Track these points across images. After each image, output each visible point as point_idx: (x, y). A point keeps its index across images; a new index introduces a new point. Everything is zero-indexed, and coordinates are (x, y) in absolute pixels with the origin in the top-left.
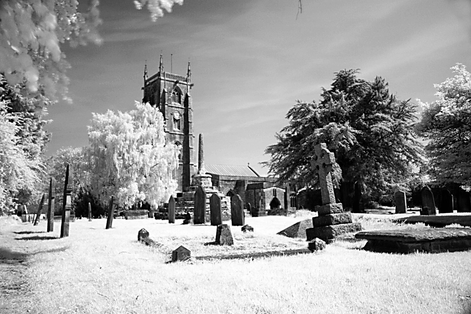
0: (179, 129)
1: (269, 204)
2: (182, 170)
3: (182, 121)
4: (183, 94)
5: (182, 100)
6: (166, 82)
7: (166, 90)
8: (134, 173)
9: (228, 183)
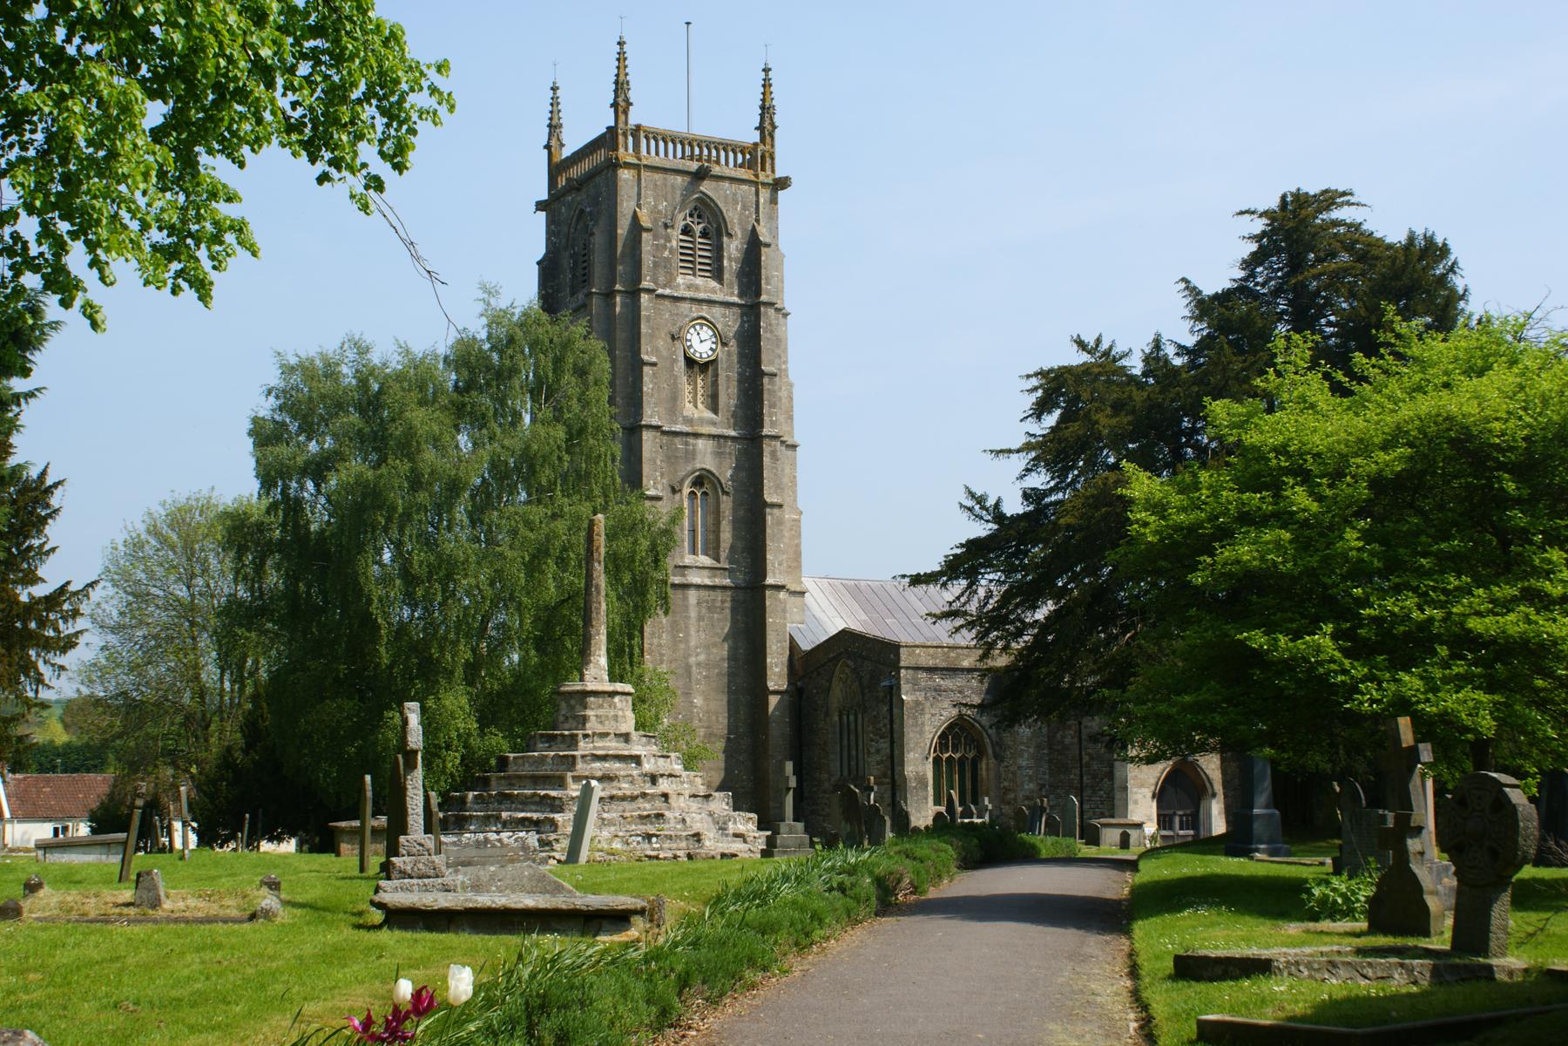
0: (715, 410)
1: (1147, 792)
2: (728, 611)
3: (729, 368)
4: (737, 230)
5: (731, 265)
6: (645, 174)
7: (645, 221)
8: (455, 643)
9: (947, 683)
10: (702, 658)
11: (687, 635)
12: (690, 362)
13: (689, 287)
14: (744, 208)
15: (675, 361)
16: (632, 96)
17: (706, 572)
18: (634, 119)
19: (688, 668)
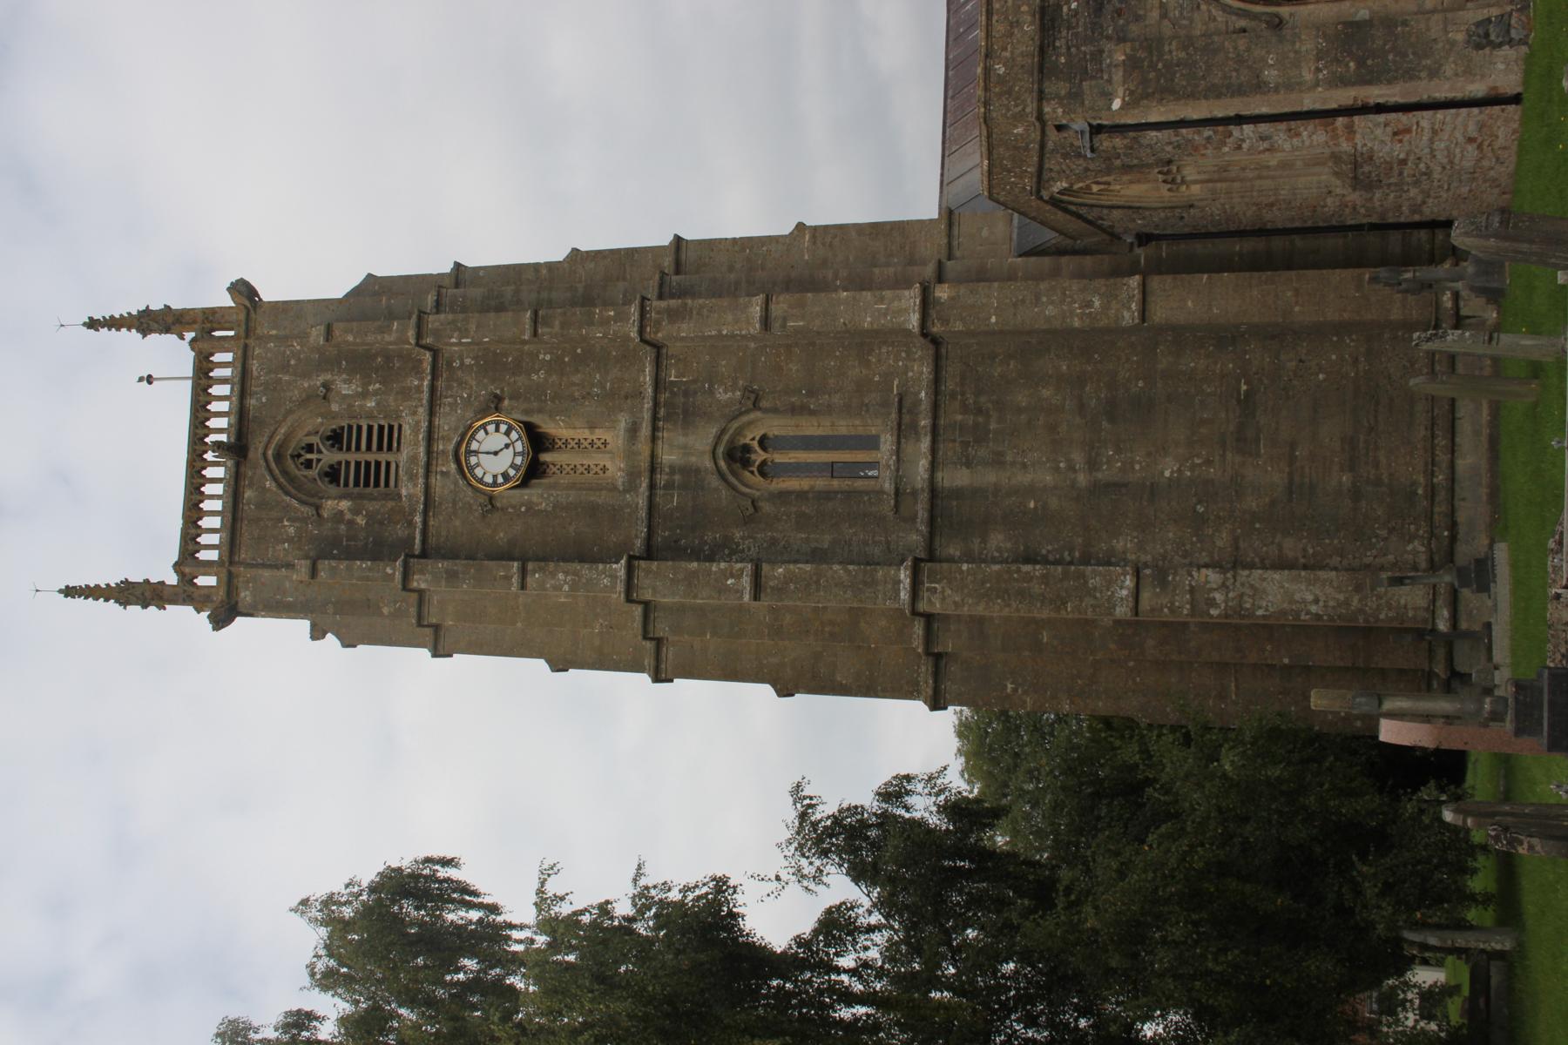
10: (1078, 457)
11: (1030, 491)
12: (533, 471)
13: (412, 477)
14: (285, 367)
15: (530, 506)
16: (136, 577)
17: (909, 448)
18: (172, 579)
19: (1098, 489)
